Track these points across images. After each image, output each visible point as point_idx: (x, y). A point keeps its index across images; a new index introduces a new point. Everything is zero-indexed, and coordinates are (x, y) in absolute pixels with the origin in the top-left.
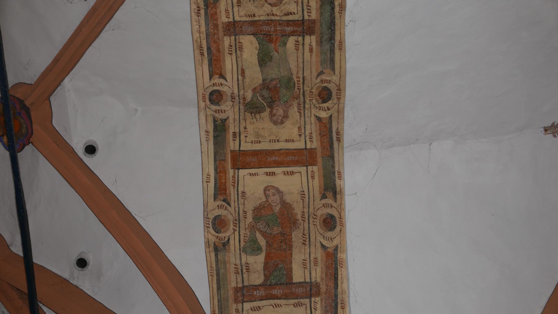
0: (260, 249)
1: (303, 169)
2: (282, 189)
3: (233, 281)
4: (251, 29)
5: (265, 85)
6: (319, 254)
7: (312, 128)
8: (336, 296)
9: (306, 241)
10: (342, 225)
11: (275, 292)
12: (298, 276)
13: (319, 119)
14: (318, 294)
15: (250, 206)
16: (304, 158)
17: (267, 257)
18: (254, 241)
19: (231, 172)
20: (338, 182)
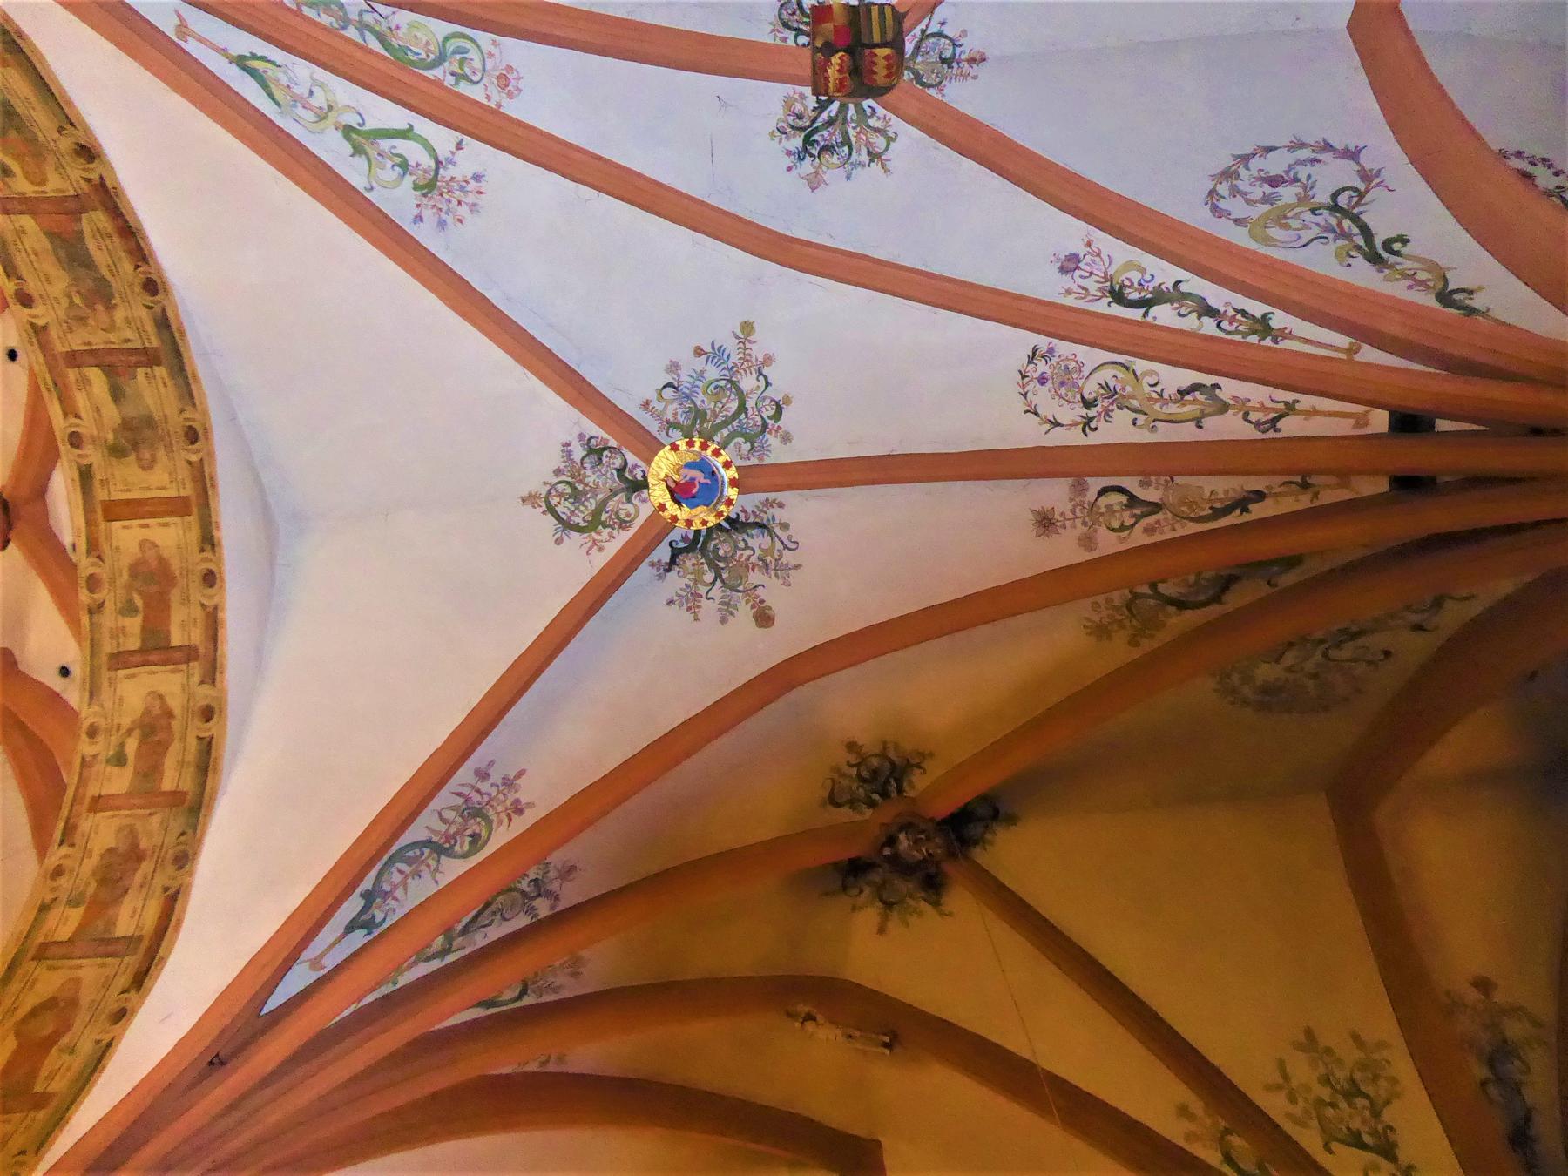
0: (136, 611)
1: (177, 520)
2: (158, 542)
3: (108, 647)
4: (92, 360)
5: (127, 425)
6: (198, 614)
7: (184, 473)
8: (215, 660)
9: (186, 601)
10: (222, 580)
11: (153, 657)
12: (177, 639)
13: (190, 463)
14: (196, 658)
15: (125, 562)
16: (177, 507)
17: (145, 619)
18: (130, 601)
19: (103, 525)
20: (215, 533)
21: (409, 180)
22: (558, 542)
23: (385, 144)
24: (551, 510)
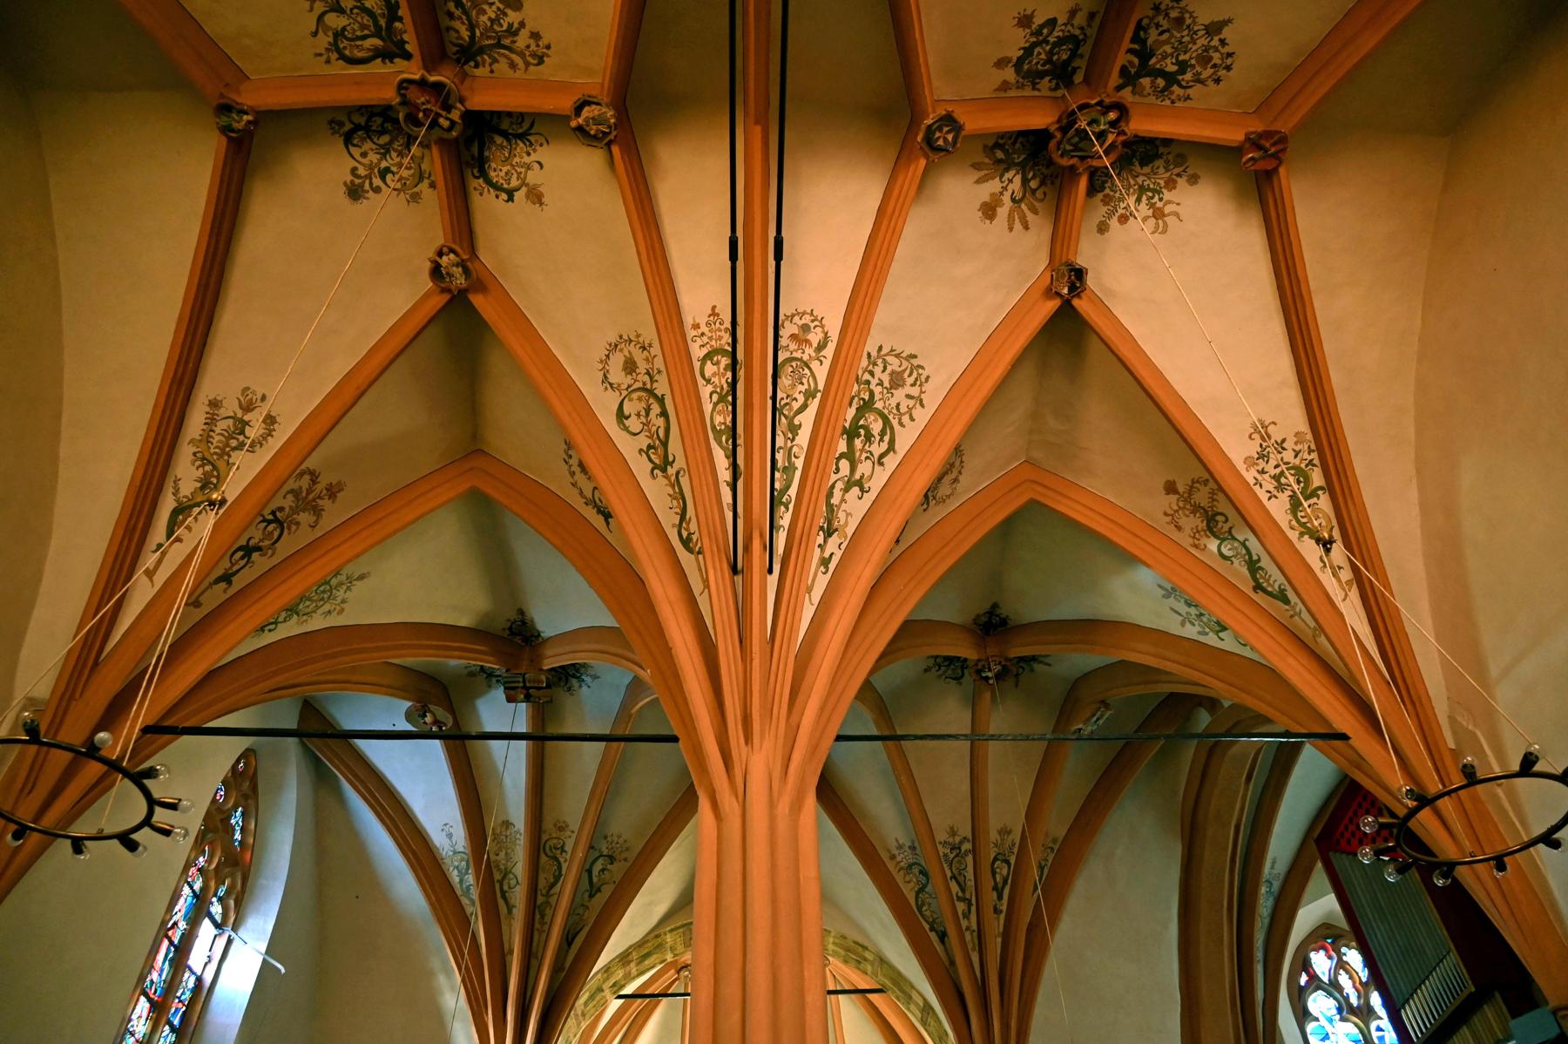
23: (595, 879)
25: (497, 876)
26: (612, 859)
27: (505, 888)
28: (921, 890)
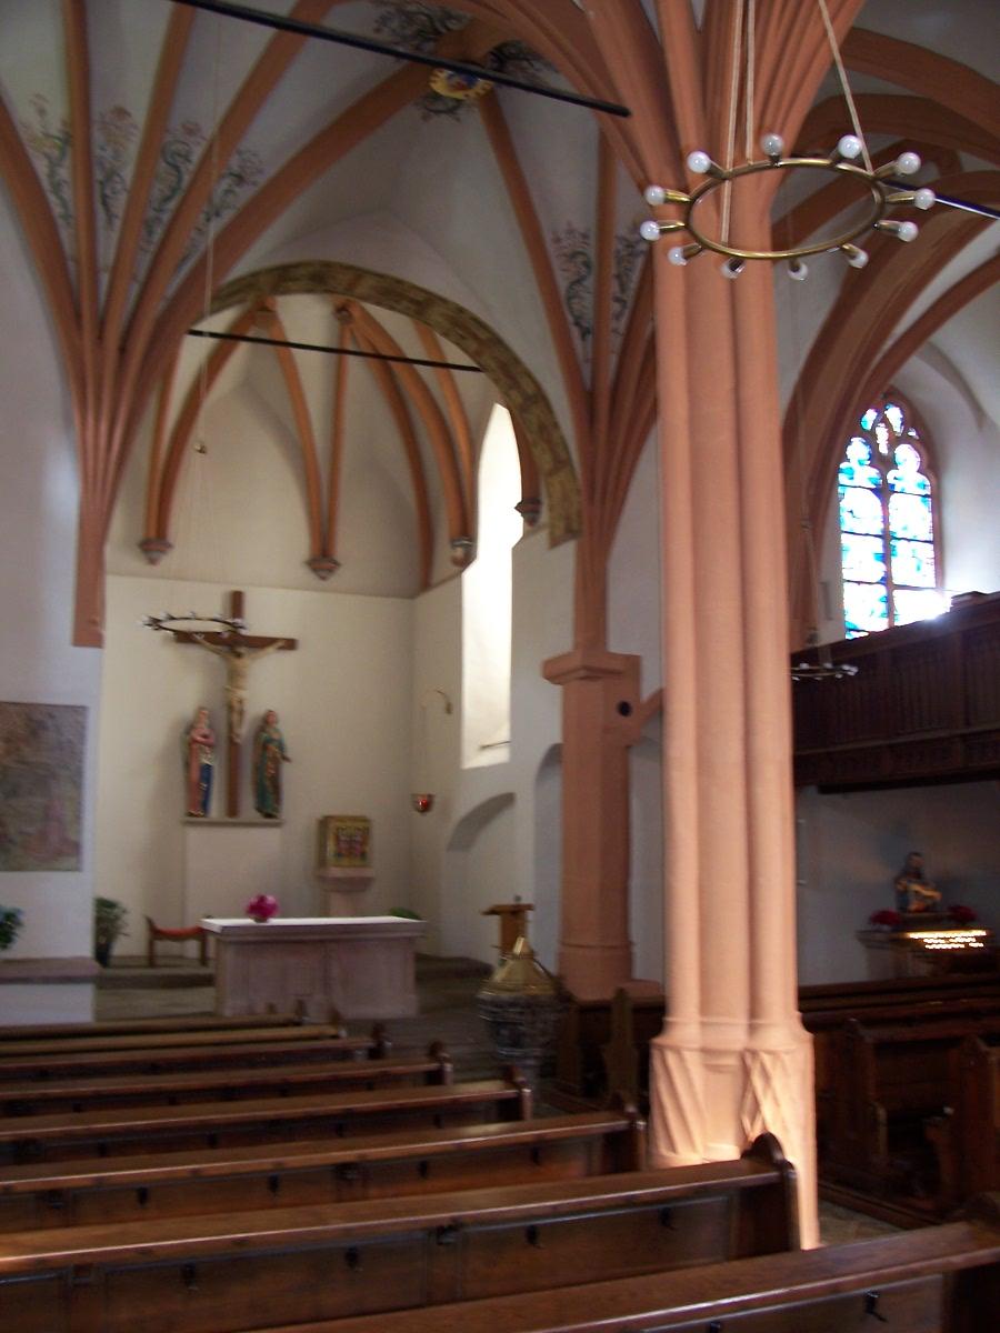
21: (237, 189)
22: (458, 120)
24: (438, 112)
25: (99, 175)
26: (240, 179)
27: (108, 192)
28: (578, 282)
